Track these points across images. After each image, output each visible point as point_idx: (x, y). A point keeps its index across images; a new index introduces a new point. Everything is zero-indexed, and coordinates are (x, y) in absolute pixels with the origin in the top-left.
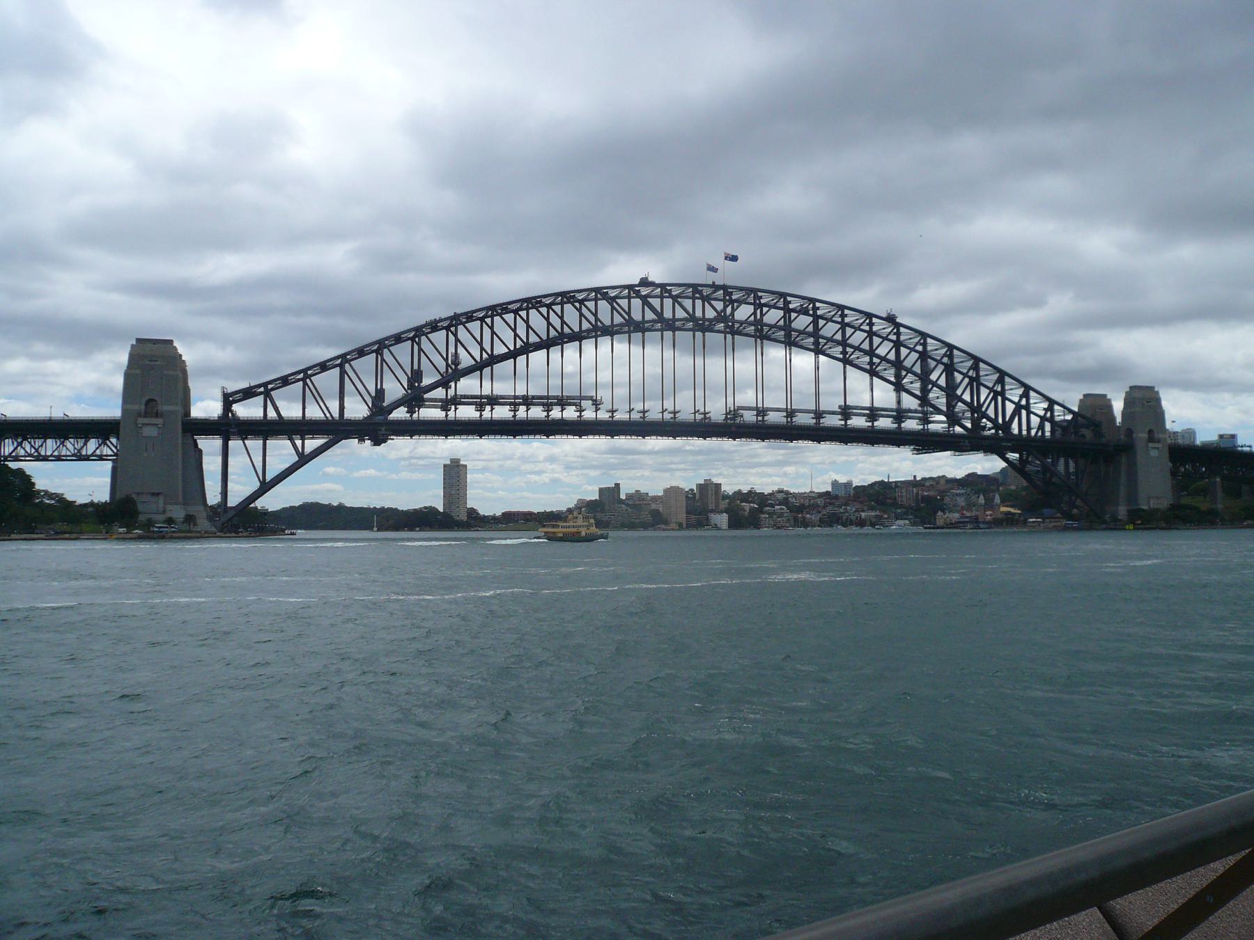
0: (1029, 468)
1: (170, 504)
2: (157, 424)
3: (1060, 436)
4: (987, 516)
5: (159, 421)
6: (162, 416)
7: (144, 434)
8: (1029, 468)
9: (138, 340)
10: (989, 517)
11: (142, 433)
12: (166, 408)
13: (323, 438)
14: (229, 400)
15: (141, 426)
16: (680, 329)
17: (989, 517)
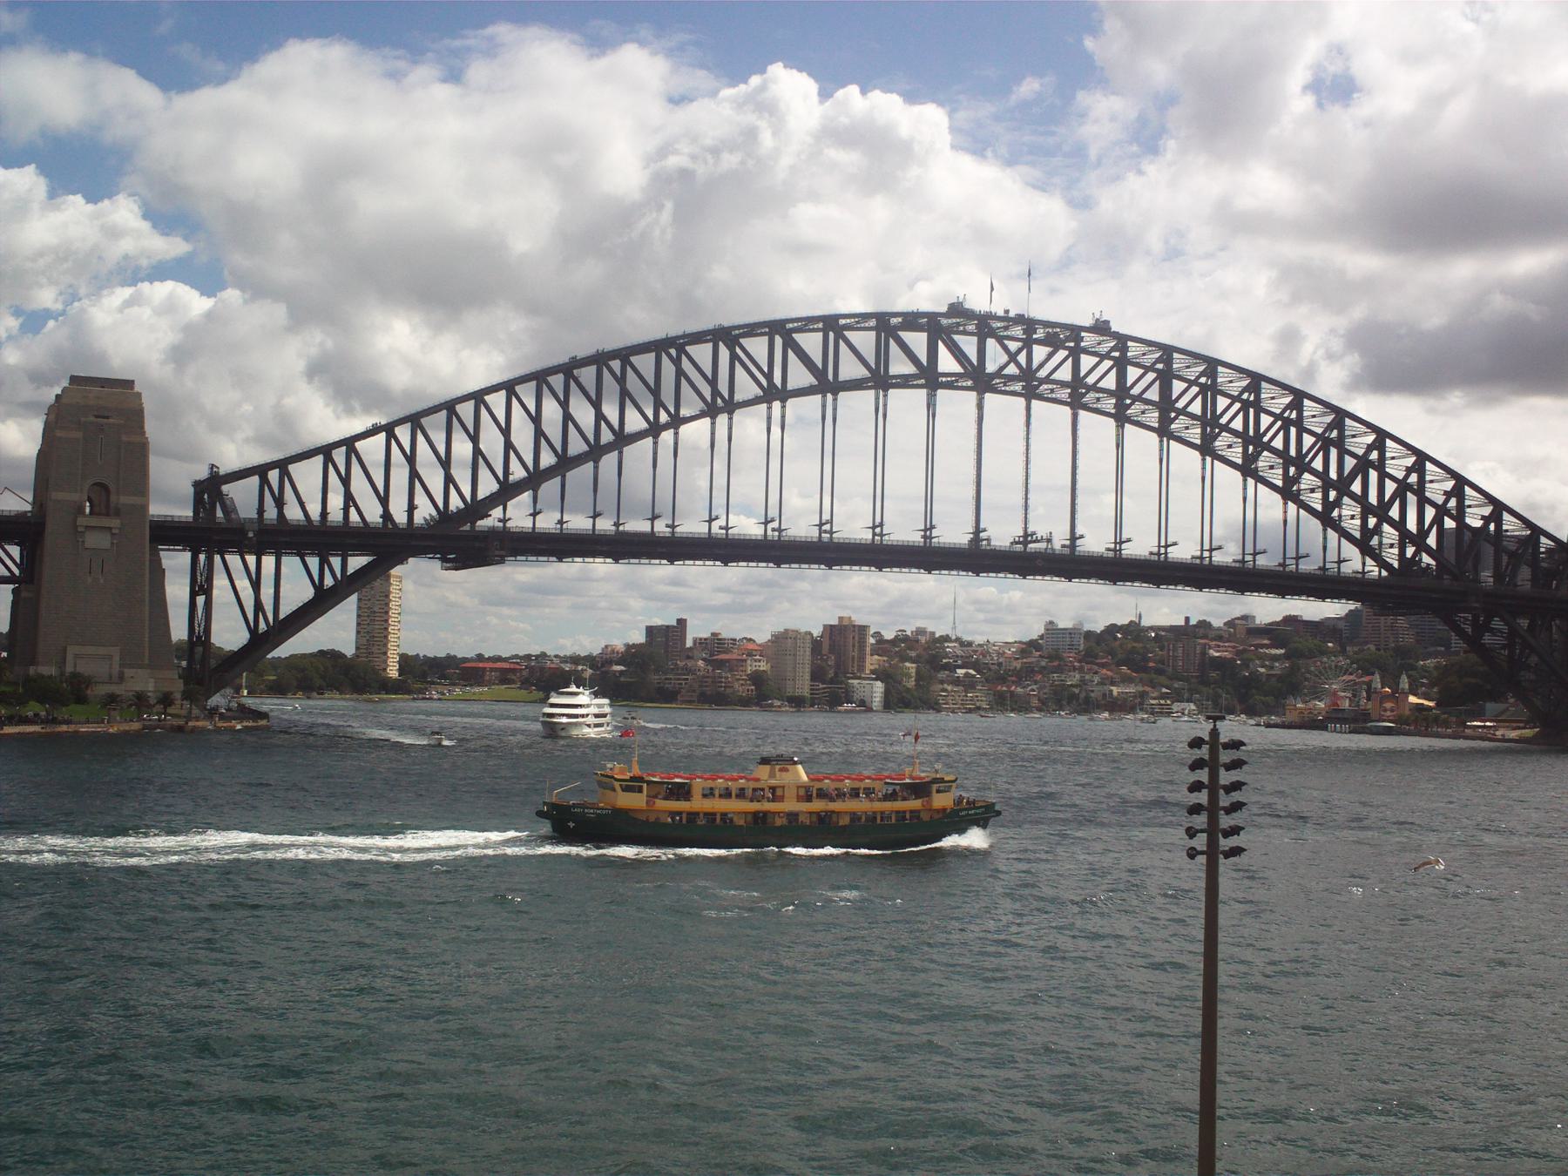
0: (1487, 639)
1: (131, 666)
2: (110, 529)
3: (1528, 585)
4: (1385, 710)
5: (115, 523)
6: (117, 513)
7: (86, 546)
8: (1487, 639)
9: (74, 380)
10: (1388, 713)
11: (83, 542)
12: (125, 500)
13: (367, 555)
14: (210, 488)
15: (80, 529)
16: (949, 386)
17: (1388, 713)
